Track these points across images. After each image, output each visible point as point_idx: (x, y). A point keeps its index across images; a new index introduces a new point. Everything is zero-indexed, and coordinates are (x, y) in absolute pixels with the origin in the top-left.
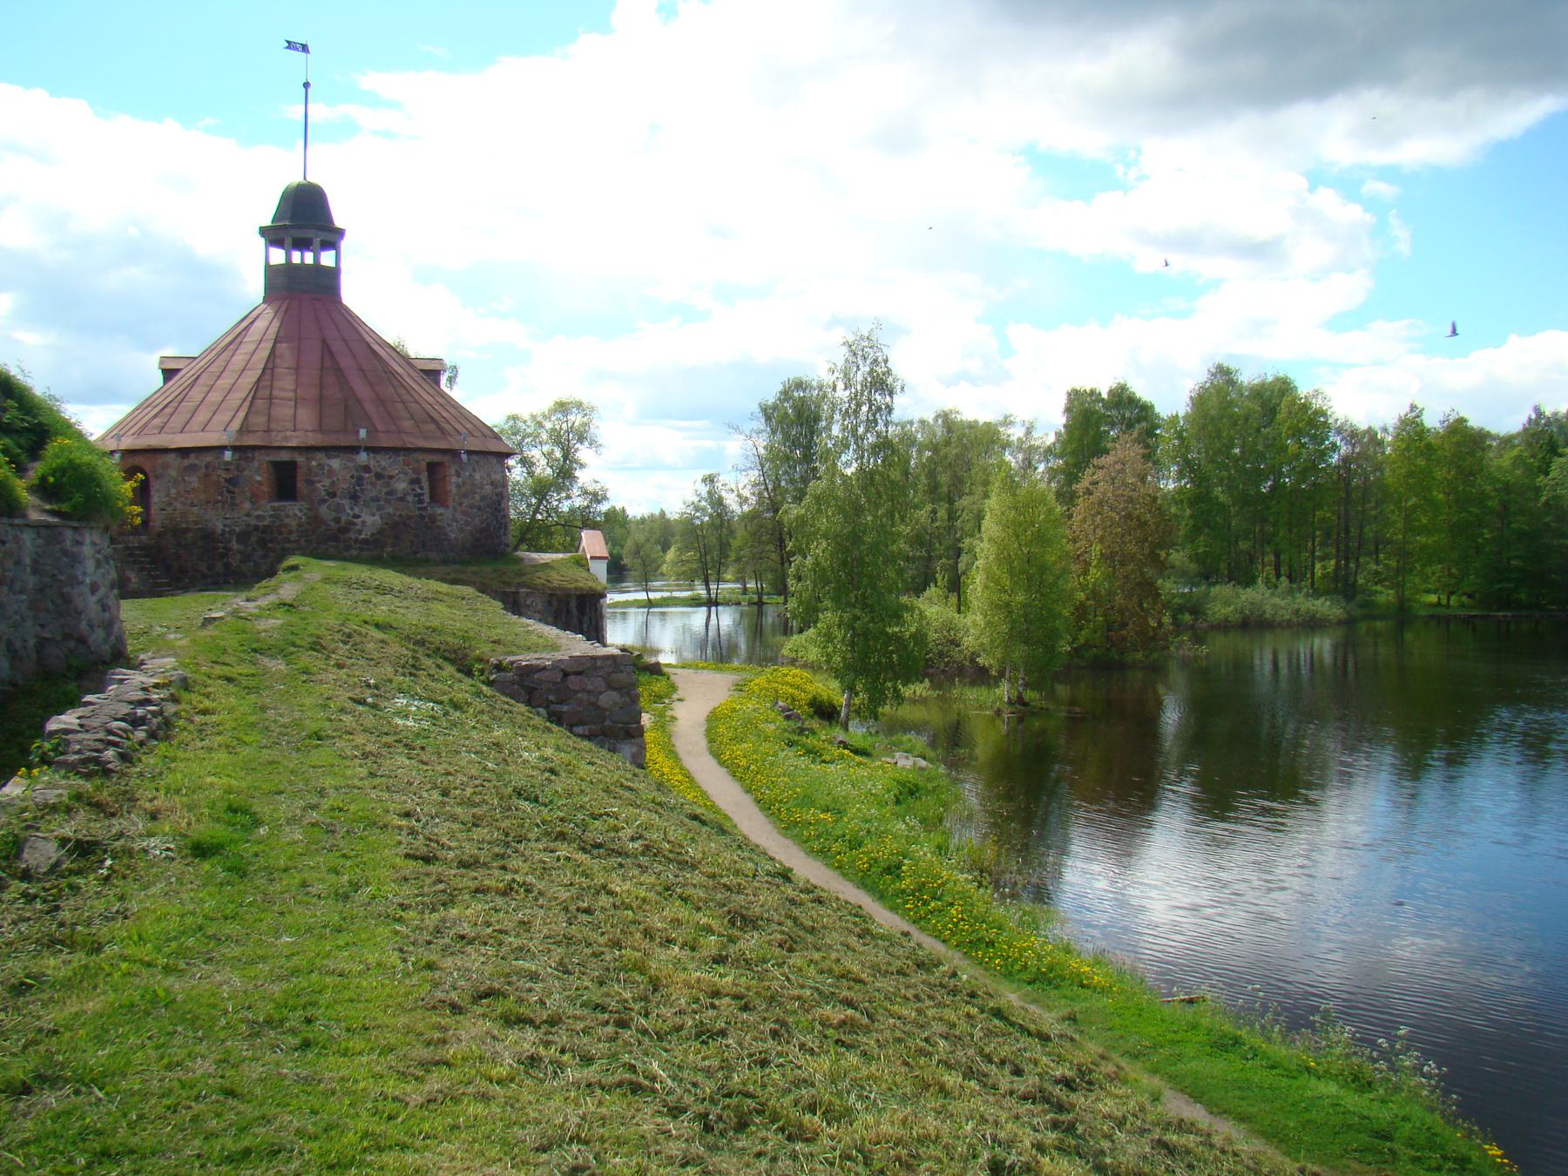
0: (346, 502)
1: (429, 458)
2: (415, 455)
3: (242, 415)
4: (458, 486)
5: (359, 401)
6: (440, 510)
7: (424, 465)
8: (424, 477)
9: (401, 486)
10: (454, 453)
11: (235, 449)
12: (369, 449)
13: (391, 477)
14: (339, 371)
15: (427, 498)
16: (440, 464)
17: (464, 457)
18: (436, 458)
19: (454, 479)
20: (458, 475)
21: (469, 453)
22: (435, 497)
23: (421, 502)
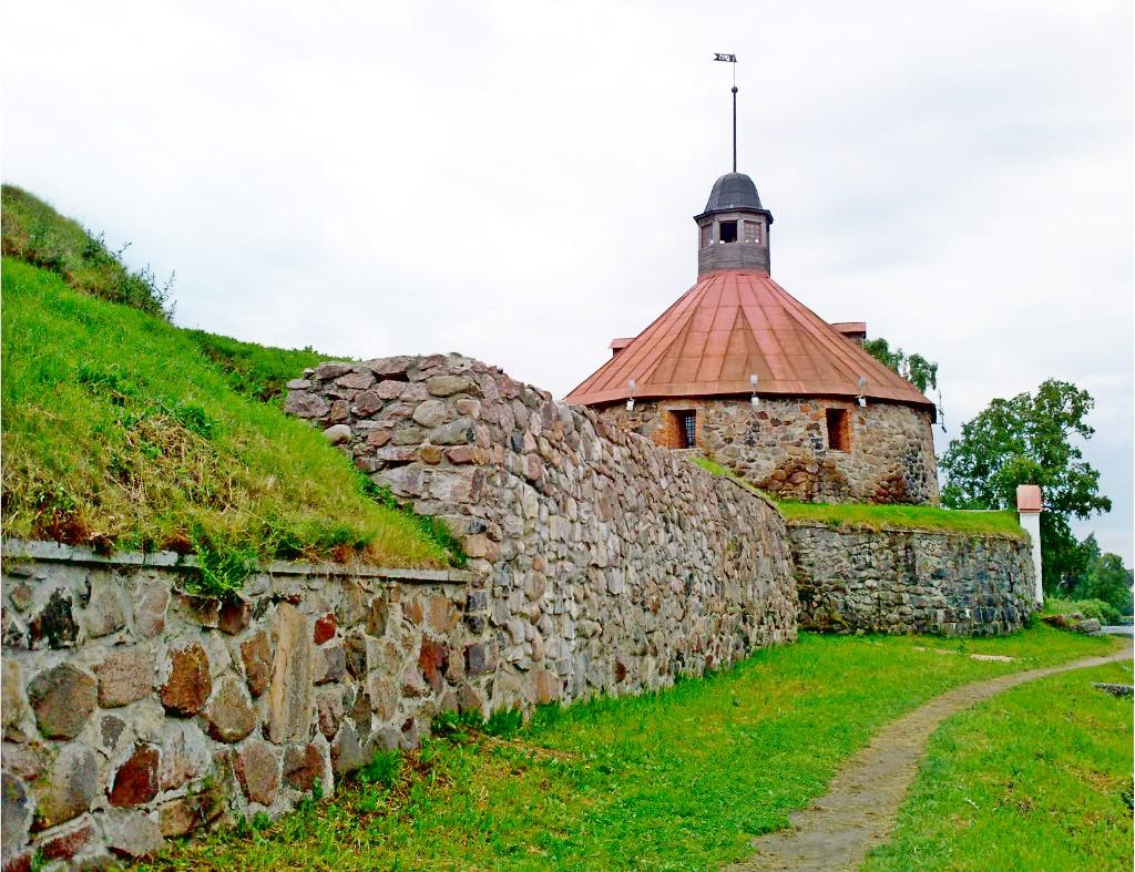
0: (742, 447)
1: (828, 405)
2: (813, 402)
3: (651, 371)
4: (863, 433)
5: (762, 355)
6: (837, 454)
7: (822, 412)
8: (823, 423)
9: (798, 431)
10: (852, 399)
11: (639, 401)
12: (764, 396)
13: (788, 423)
14: (748, 329)
15: (825, 443)
16: (843, 412)
17: (863, 402)
18: (836, 405)
19: (857, 426)
20: (862, 422)
21: (872, 401)
22: (835, 443)
23: (818, 447)
